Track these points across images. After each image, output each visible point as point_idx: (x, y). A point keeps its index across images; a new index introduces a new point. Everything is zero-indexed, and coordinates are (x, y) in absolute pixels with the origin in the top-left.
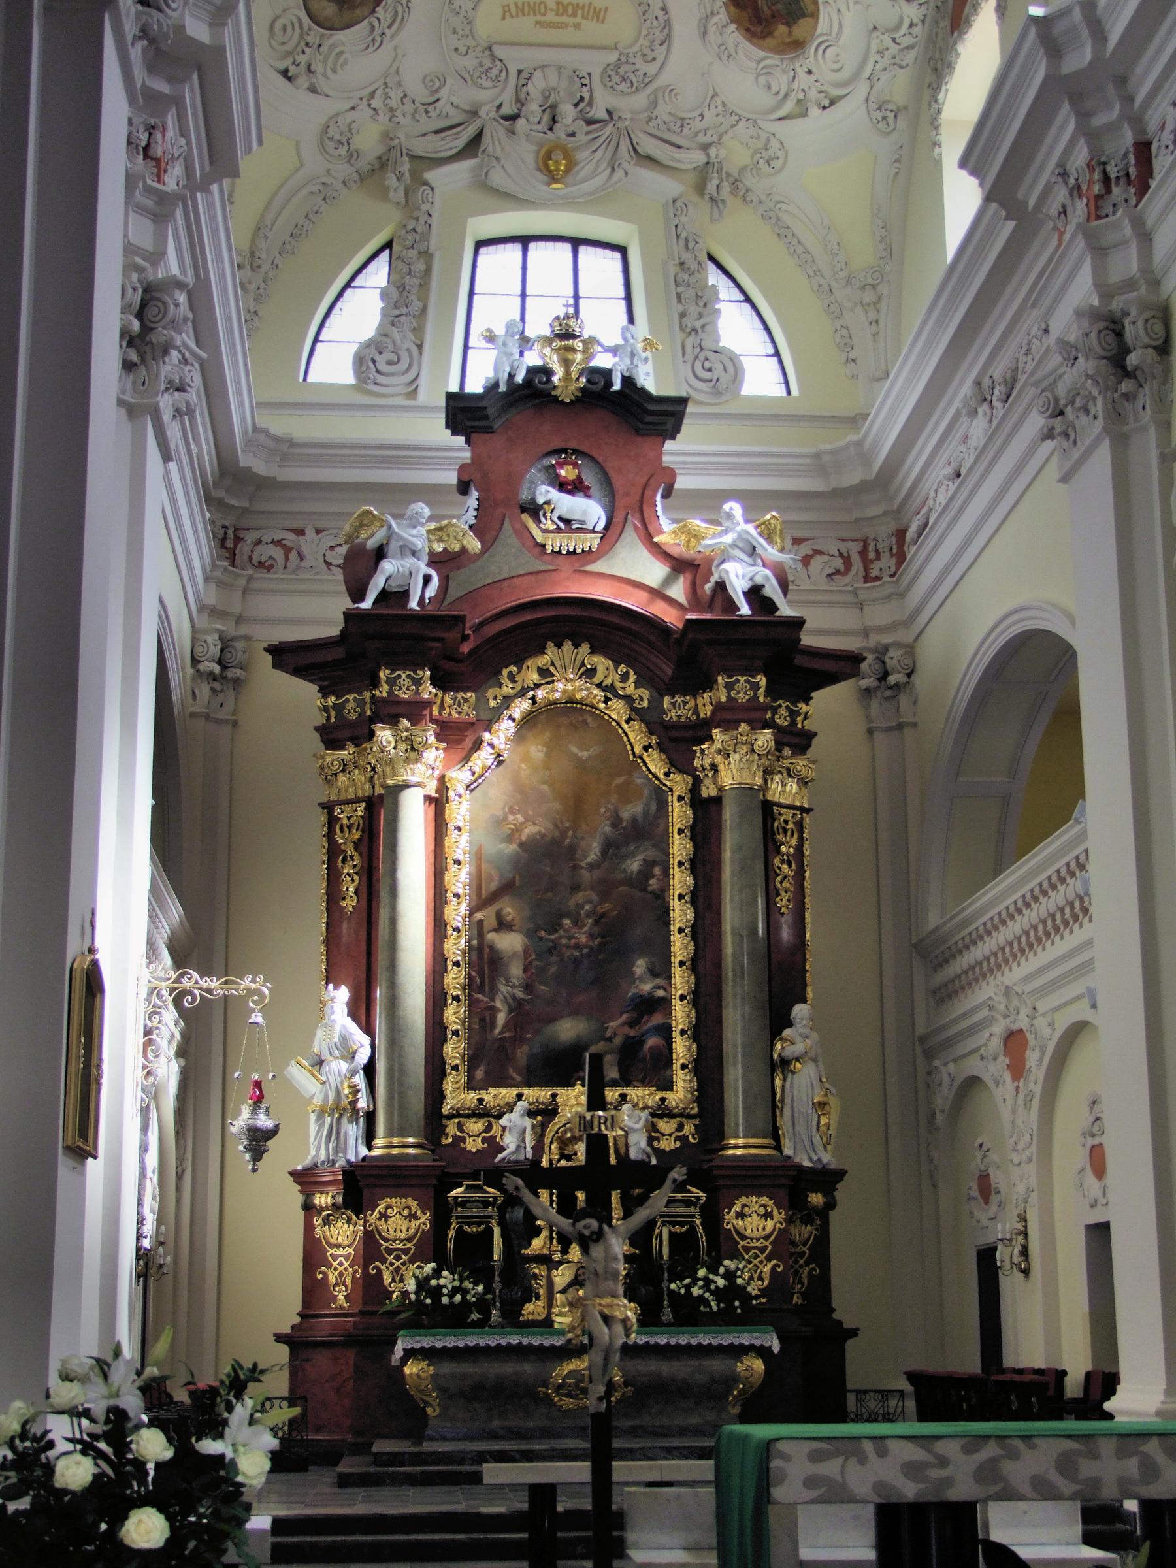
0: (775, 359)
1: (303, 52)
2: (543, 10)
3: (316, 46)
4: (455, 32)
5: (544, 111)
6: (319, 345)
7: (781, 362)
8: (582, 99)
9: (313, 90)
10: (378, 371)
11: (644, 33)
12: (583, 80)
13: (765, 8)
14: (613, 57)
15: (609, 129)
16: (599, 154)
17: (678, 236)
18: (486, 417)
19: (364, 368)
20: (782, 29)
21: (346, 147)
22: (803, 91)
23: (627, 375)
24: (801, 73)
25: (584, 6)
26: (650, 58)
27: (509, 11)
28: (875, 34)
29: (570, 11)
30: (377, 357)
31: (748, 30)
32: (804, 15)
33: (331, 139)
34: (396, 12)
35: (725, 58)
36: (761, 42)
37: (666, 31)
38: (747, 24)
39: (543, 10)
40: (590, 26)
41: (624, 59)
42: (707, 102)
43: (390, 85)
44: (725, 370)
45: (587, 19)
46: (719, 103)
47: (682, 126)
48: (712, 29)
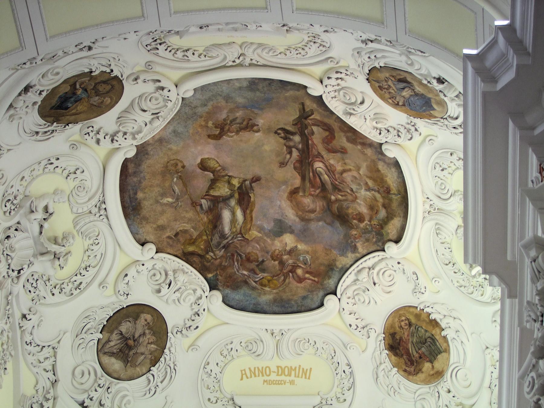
1: (96, 391)
2: (268, 373)
4: (208, 388)
11: (337, 383)
13: (415, 353)
20: (427, 366)
24: (443, 393)
25: (295, 368)
26: (342, 400)
27: (246, 374)
28: (488, 351)
29: (286, 373)
31: (405, 371)
32: (440, 352)
34: (166, 372)
35: (392, 393)
36: (415, 378)
37: (351, 380)
38: (404, 367)
39: (268, 373)
41: (324, 402)
45: (298, 377)
48: (381, 374)
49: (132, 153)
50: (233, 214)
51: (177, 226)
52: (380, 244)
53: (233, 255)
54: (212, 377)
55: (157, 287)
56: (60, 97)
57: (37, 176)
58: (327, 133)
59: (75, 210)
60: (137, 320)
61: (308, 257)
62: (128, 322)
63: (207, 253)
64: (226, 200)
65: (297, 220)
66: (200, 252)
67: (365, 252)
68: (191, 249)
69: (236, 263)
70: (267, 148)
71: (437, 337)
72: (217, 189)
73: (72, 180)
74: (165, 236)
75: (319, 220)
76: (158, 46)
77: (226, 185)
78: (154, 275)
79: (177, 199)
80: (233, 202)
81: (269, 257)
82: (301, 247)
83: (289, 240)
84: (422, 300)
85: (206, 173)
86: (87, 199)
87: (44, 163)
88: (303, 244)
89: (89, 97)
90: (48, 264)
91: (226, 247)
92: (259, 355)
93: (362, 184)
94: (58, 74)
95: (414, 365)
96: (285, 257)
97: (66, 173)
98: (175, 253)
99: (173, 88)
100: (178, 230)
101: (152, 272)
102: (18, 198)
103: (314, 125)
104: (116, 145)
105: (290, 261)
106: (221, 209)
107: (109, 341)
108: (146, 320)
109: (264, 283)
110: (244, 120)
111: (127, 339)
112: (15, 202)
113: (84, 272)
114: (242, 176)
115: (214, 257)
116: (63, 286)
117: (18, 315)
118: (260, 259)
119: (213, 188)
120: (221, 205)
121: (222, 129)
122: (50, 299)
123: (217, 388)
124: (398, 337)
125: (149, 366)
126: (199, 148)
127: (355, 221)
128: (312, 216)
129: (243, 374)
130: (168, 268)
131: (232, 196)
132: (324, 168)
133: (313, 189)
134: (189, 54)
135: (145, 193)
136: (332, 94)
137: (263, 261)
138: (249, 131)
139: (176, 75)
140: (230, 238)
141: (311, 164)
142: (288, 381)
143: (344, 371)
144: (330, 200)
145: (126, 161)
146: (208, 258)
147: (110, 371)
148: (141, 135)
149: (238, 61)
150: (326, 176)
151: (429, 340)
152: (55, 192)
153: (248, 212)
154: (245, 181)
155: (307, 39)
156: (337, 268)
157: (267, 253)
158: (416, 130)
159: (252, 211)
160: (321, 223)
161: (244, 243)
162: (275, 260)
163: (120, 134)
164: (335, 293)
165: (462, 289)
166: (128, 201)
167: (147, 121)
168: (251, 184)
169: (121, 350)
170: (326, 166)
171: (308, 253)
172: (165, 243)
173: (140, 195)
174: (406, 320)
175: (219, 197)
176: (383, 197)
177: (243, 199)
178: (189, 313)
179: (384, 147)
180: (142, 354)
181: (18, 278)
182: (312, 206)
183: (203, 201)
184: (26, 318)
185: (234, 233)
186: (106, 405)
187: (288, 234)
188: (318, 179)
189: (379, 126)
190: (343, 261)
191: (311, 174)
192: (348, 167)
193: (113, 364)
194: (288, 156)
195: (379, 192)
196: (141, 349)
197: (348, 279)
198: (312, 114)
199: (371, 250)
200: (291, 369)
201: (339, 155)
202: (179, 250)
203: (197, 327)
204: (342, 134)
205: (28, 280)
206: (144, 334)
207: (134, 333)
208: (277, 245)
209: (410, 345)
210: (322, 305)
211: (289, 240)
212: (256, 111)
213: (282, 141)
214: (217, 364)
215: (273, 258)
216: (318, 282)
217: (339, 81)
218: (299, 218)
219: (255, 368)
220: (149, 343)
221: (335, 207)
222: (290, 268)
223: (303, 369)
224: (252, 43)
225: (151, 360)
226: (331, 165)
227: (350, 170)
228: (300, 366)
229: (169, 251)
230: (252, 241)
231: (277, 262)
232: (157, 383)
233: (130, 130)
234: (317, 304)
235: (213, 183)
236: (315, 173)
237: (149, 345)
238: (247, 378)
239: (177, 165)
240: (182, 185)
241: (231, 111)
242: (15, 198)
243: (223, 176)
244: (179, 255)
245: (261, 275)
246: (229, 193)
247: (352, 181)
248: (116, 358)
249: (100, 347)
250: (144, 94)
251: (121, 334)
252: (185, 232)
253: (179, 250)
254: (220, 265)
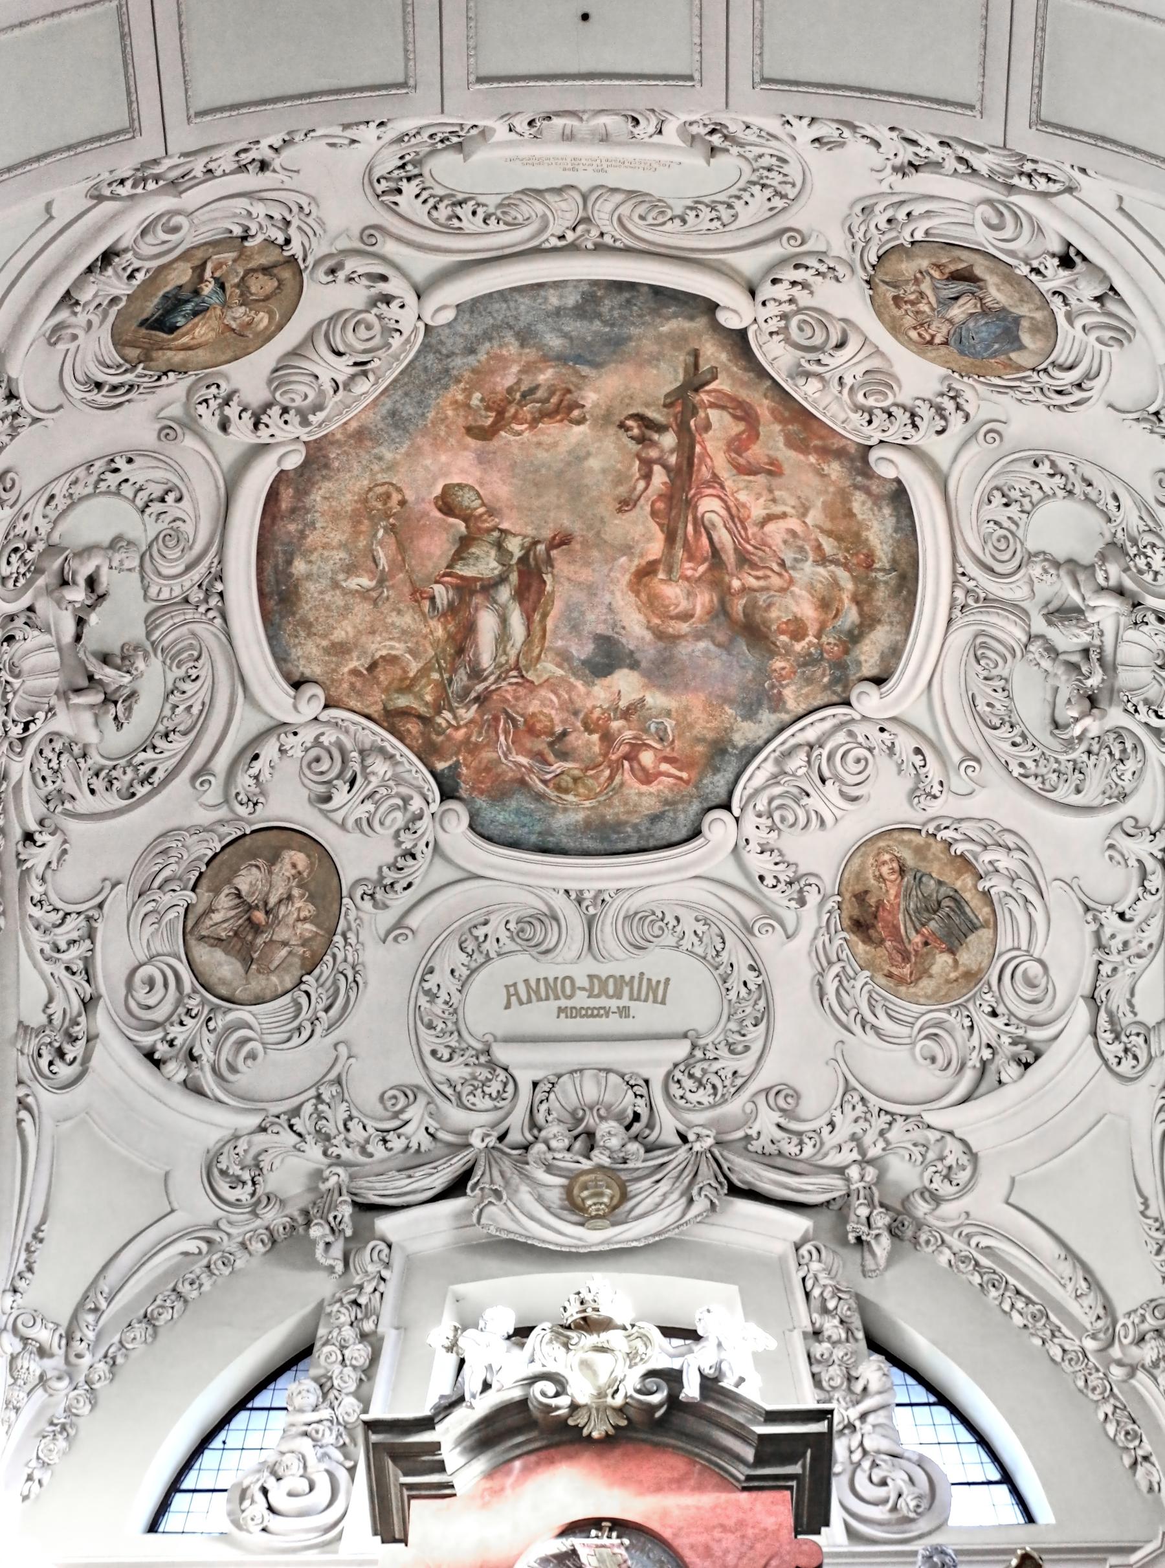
0: (1004, 1489)
1: (181, 1023)
2: (568, 991)
3: (203, 1017)
4: (430, 1026)
5: (576, 1138)
6: (179, 1500)
7: (1015, 1491)
8: (637, 1117)
9: (193, 1088)
10: (270, 1509)
12: (640, 1086)
14: (681, 1050)
15: (682, 1153)
16: (664, 1187)
17: (807, 1295)
18: (440, 1467)
19: (247, 1503)
21: (249, 1188)
22: (989, 1046)
23: (708, 1372)
24: (983, 1021)
25: (633, 977)
26: (740, 1048)
27: (517, 994)
29: (611, 990)
30: (271, 1483)
32: (974, 928)
33: (223, 1173)
34: (337, 990)
37: (762, 1004)
38: (887, 967)
39: (568, 991)
40: (646, 1016)
42: (837, 1102)
43: (326, 1097)
44: (911, 1480)
45: (638, 999)
46: (857, 1098)
47: (801, 1143)
49: (293, 462)
50: (504, 621)
51: (374, 647)
52: (839, 689)
53: (496, 719)
54: (440, 1001)
55: (322, 789)
56: (165, 296)
57: (82, 499)
58: (742, 426)
59: (153, 591)
60: (273, 864)
61: (669, 724)
62: (254, 870)
63: (439, 713)
64: (489, 587)
65: (648, 636)
66: (423, 710)
67: (801, 710)
68: (402, 702)
69: (502, 738)
70: (594, 463)
71: (967, 896)
72: (471, 561)
73: (154, 517)
74: (346, 670)
75: (698, 636)
76: (404, 185)
77: (493, 553)
78: (318, 760)
79: (381, 582)
80: (504, 594)
81: (579, 724)
84: (931, 813)
85: (451, 520)
86: (180, 568)
87: (99, 466)
88: (658, 694)
89: (225, 305)
90: (87, 717)
91: (482, 700)
92: (547, 952)
93: (807, 548)
94: (176, 229)
95: (909, 961)
96: (615, 725)
97: (143, 496)
98: (367, 711)
99: (410, 299)
100: (377, 656)
101: (313, 753)
102: (39, 547)
103: (713, 405)
104: (264, 435)
105: (628, 734)
106: (476, 609)
107: (210, 910)
108: (294, 866)
109: (563, 784)
110: (552, 393)
111: (250, 908)
112: (29, 556)
113: (161, 744)
114: (530, 531)
115: (454, 723)
116: (114, 774)
117: (18, 834)
118: (559, 729)
119: (462, 559)
120: (477, 599)
121: (501, 413)
122: (85, 803)
123: (451, 1027)
124: (872, 901)
125: (299, 974)
126: (443, 458)
127: (784, 638)
128: (684, 627)
129: (511, 990)
130: (348, 744)
131: (502, 579)
132: (723, 513)
133: (691, 565)
134: (464, 212)
135: (310, 562)
136: (774, 325)
137: (564, 734)
138: (561, 421)
139: (423, 265)
140: (492, 678)
141: (691, 505)
142: (614, 1009)
143: (745, 984)
144: (729, 587)
145: (281, 477)
146: (439, 725)
147: (213, 980)
148: (321, 416)
149: (570, 236)
150: (724, 532)
151: (946, 902)
152: (115, 544)
153: (537, 617)
154: (535, 543)
155: (748, 175)
156: (734, 747)
157: (576, 713)
158: (958, 407)
159: (545, 616)
160: (702, 645)
161: (522, 691)
162: (591, 732)
163: (275, 411)
164: (727, 807)
165: (1030, 781)
166: (272, 579)
167: (341, 379)
168: (548, 551)
169: (236, 934)
170: (728, 509)
171: (668, 714)
172: (345, 686)
173: (299, 567)
174: (892, 860)
175: (475, 579)
176: (855, 579)
177: (528, 587)
178: (389, 853)
179: (873, 456)
180: (285, 944)
181: (22, 740)
182: (684, 605)
183: (439, 590)
184: (34, 842)
185: (502, 666)
186: (204, 1058)
187: (626, 671)
188: (705, 541)
189: (871, 402)
191: (690, 528)
192: (778, 509)
193: (220, 964)
194: (641, 484)
195: (845, 566)
196: (283, 934)
197: (759, 772)
198: (715, 378)
199: (816, 703)
200: (620, 981)
201: (761, 479)
202: (376, 703)
203: (410, 885)
204: (777, 427)
205: (41, 752)
206: (289, 897)
207: (268, 894)
209: (901, 917)
210: (696, 833)
212: (585, 370)
213: (634, 447)
214: (452, 972)
215: (588, 729)
216: (687, 782)
217: (796, 291)
218: (654, 633)
219: (538, 980)
220: (298, 920)
221: (738, 606)
222: (625, 749)
223: (649, 980)
224: (614, 190)
225: (303, 958)
226: (741, 505)
227: (784, 515)
228: (642, 974)
229: (352, 704)
230: (541, 685)
231: (595, 737)
232: (315, 1012)
233: (299, 402)
234: (684, 833)
235: (465, 543)
236: (699, 523)
237: (299, 924)
238: (521, 1003)
239: (388, 496)
240: (394, 547)
241: (527, 369)
242: (29, 547)
243: (489, 531)
244: (376, 716)
245: (558, 766)
246: (496, 572)
247: (785, 542)
248: (227, 953)
249: (190, 924)
250: (340, 314)
251: (239, 895)
252: (392, 660)
253: (376, 703)
254: (467, 740)
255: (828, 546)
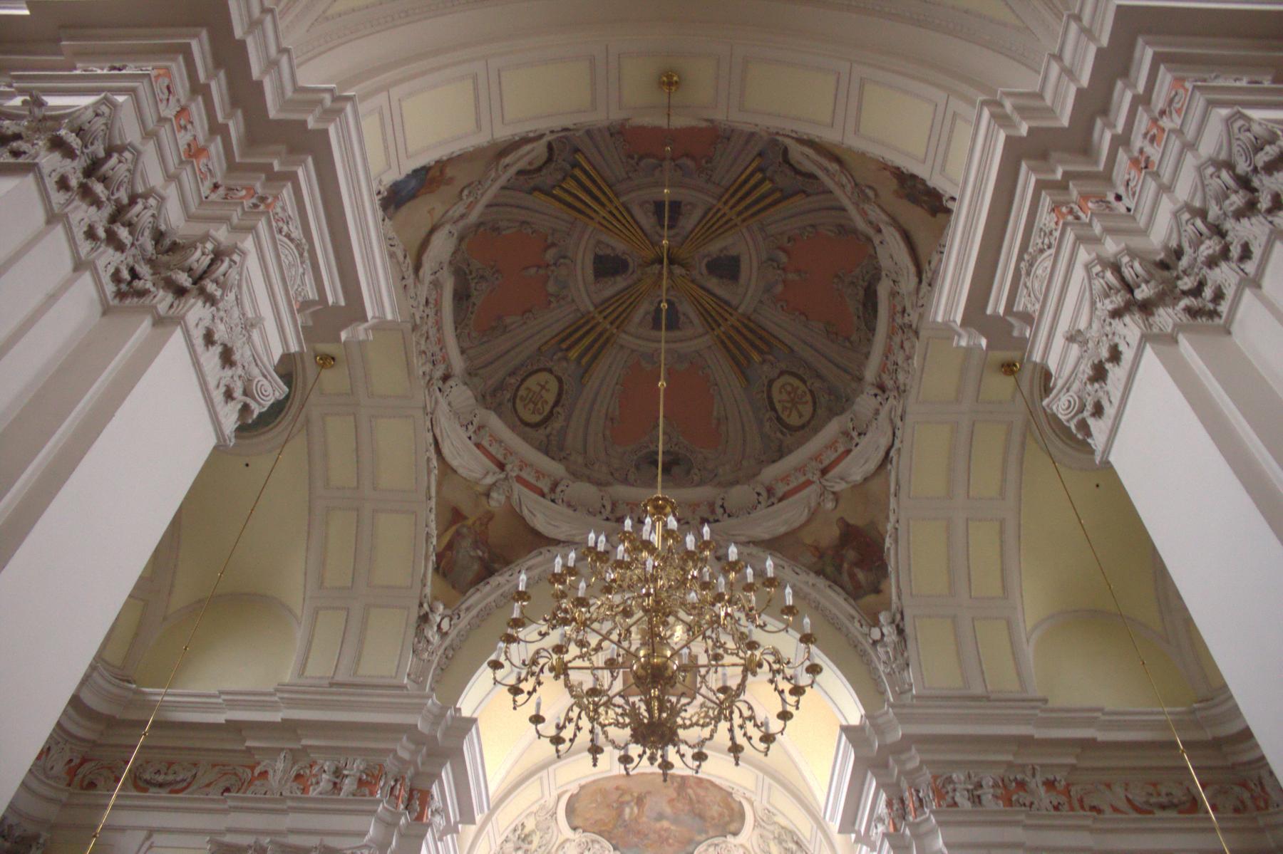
50: (632, 809)
61: (677, 834)
68: (603, 828)
80: (632, 804)
82: (673, 828)
83: (665, 824)
91: (625, 827)
131: (632, 801)
190: (699, 838)
208: (658, 825)
211: (665, 824)
235: (621, 795)
245: (646, 841)
252: (601, 820)
255: (722, 804)
